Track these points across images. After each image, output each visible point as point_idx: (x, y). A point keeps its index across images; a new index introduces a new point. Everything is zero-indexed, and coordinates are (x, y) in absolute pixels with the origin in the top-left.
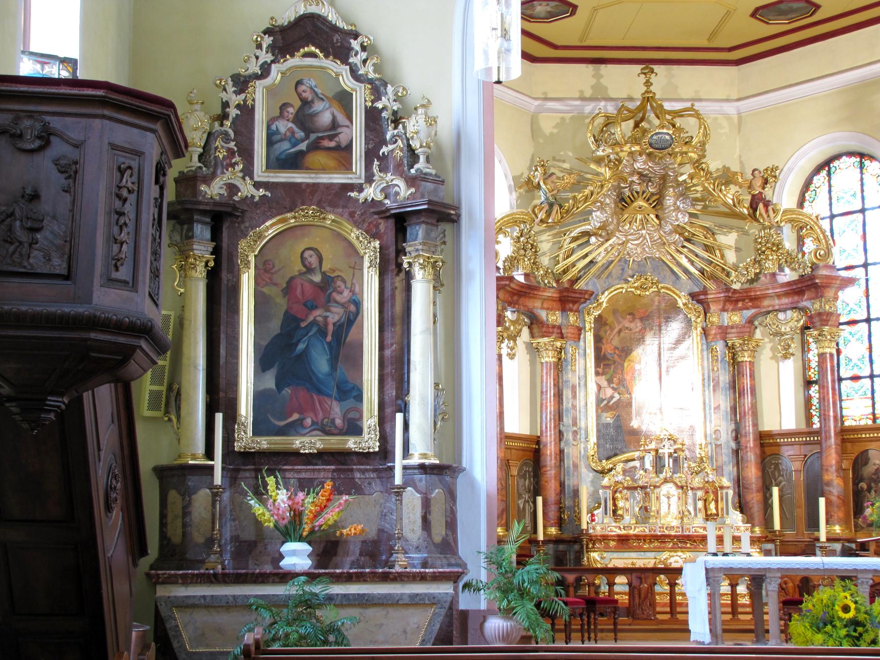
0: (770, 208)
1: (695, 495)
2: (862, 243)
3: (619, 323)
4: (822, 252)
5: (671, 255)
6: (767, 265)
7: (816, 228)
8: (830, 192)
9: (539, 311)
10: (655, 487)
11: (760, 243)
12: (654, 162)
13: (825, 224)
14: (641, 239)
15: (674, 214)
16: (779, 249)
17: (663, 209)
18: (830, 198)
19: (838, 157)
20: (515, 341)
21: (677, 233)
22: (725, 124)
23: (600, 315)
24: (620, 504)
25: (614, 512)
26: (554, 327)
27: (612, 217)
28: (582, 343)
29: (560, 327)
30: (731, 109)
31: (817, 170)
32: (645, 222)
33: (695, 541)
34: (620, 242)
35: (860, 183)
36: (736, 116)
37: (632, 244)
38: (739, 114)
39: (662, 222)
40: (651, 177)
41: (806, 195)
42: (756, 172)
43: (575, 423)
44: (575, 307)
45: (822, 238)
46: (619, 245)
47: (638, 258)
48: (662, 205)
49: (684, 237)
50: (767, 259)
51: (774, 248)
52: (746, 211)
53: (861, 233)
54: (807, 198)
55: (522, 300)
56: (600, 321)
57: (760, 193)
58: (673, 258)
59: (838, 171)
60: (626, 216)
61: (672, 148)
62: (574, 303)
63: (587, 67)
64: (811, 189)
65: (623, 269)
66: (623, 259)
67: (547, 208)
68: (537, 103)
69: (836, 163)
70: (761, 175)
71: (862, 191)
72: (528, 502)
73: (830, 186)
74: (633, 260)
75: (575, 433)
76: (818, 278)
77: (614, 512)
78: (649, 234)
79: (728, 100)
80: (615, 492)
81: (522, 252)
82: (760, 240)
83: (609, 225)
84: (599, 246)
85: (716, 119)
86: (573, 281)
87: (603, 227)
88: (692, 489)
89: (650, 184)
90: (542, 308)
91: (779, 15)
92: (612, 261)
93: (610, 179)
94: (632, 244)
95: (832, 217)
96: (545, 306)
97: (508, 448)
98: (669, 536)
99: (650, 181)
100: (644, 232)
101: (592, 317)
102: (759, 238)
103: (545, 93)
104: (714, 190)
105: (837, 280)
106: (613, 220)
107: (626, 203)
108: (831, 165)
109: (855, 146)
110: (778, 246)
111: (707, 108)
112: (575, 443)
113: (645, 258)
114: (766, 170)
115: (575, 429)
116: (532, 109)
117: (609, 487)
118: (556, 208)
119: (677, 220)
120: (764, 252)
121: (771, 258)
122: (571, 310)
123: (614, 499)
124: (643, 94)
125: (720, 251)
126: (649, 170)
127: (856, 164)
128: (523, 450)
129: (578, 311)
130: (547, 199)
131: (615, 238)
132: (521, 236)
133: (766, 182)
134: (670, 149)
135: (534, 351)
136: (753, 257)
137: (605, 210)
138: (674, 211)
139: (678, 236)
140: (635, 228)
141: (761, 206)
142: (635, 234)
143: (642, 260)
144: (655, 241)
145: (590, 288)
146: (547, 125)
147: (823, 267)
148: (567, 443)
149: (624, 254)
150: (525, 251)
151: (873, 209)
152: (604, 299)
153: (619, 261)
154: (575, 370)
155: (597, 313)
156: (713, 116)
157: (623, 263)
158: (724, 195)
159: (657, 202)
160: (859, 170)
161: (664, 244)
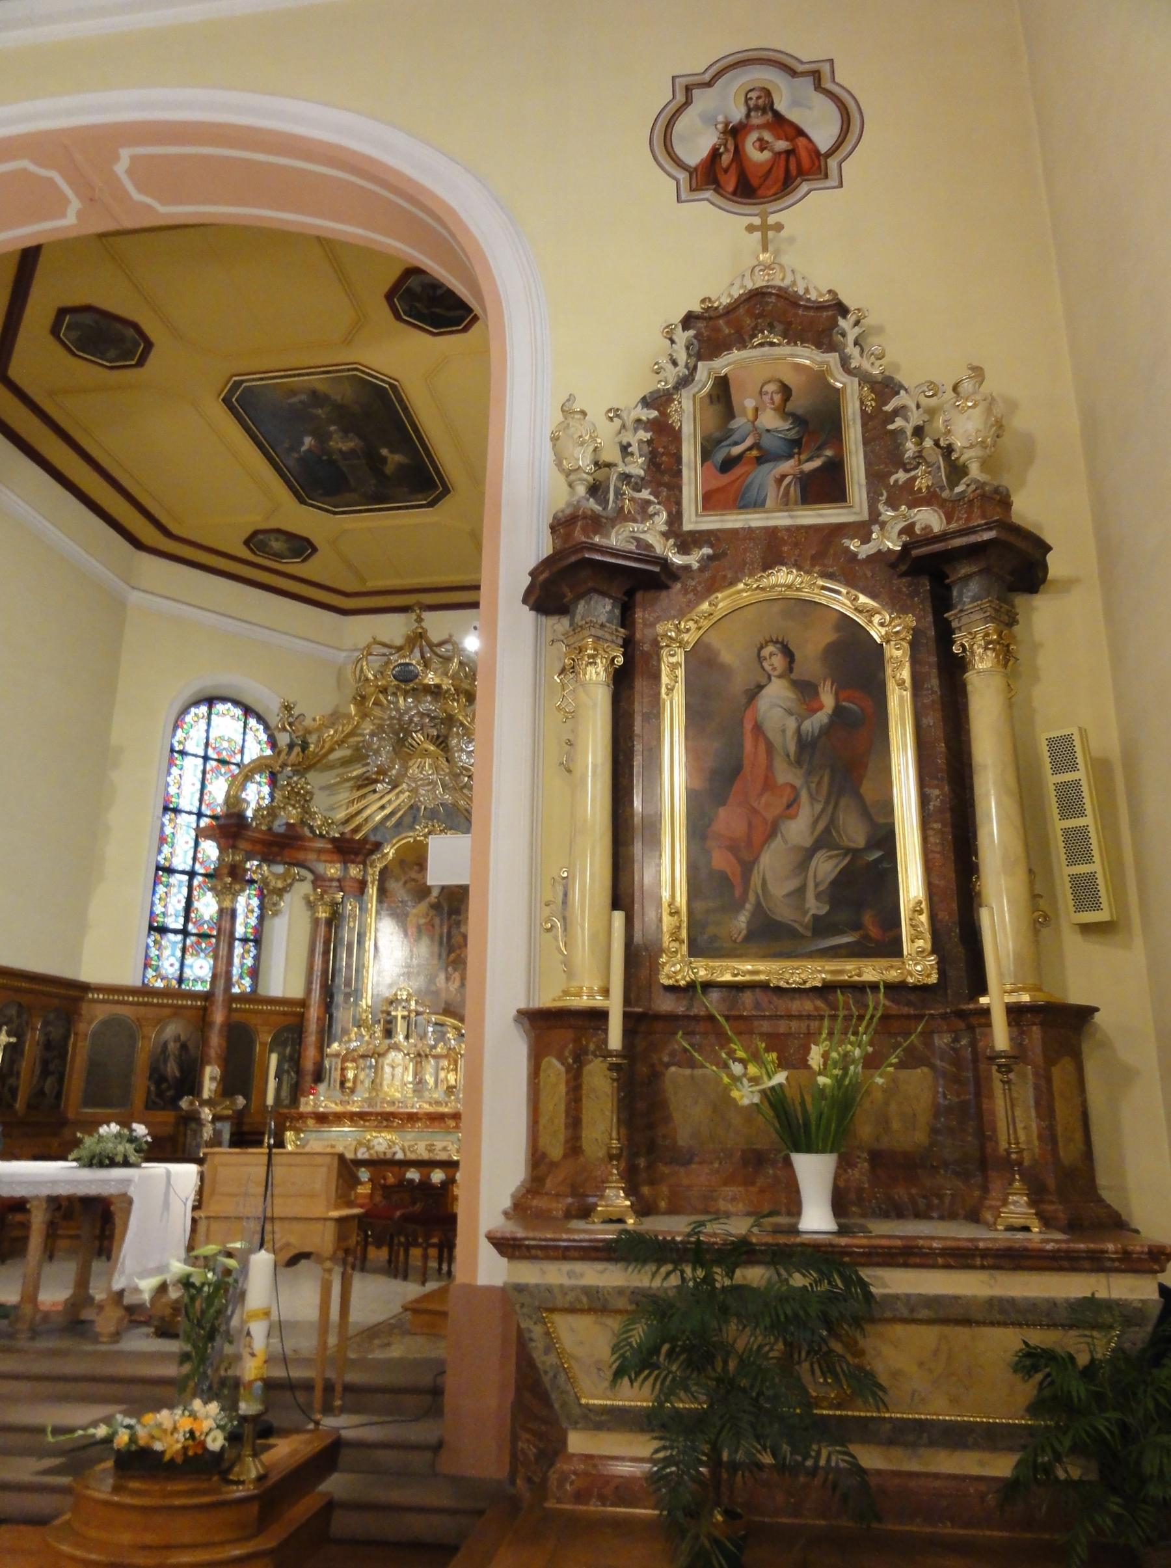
1: (437, 1064)
3: (405, 873)
9: (314, 863)
10: (380, 1055)
20: (281, 896)
21: (465, 776)
23: (386, 867)
24: (350, 1074)
25: (342, 1083)
26: (331, 880)
28: (365, 897)
29: (339, 880)
32: (437, 769)
33: (401, 1119)
43: (348, 984)
44: (360, 858)
55: (286, 852)
56: (383, 872)
62: (357, 854)
65: (415, 818)
68: (344, 654)
72: (288, 1072)
75: (347, 996)
77: (342, 1083)
80: (344, 1060)
84: (388, 793)
86: (356, 830)
88: (435, 1057)
90: (318, 860)
96: (323, 857)
97: (230, 1010)
98: (370, 1114)
101: (378, 870)
112: (346, 1006)
115: (348, 990)
117: (337, 1055)
118: (297, 749)
119: (461, 761)
122: (353, 862)
123: (343, 1069)
128: (284, 1014)
129: (364, 864)
134: (417, 680)
135: (311, 905)
138: (458, 751)
139: (466, 779)
145: (378, 838)
148: (337, 1007)
152: (390, 851)
153: (411, 807)
154: (354, 927)
155: (379, 866)
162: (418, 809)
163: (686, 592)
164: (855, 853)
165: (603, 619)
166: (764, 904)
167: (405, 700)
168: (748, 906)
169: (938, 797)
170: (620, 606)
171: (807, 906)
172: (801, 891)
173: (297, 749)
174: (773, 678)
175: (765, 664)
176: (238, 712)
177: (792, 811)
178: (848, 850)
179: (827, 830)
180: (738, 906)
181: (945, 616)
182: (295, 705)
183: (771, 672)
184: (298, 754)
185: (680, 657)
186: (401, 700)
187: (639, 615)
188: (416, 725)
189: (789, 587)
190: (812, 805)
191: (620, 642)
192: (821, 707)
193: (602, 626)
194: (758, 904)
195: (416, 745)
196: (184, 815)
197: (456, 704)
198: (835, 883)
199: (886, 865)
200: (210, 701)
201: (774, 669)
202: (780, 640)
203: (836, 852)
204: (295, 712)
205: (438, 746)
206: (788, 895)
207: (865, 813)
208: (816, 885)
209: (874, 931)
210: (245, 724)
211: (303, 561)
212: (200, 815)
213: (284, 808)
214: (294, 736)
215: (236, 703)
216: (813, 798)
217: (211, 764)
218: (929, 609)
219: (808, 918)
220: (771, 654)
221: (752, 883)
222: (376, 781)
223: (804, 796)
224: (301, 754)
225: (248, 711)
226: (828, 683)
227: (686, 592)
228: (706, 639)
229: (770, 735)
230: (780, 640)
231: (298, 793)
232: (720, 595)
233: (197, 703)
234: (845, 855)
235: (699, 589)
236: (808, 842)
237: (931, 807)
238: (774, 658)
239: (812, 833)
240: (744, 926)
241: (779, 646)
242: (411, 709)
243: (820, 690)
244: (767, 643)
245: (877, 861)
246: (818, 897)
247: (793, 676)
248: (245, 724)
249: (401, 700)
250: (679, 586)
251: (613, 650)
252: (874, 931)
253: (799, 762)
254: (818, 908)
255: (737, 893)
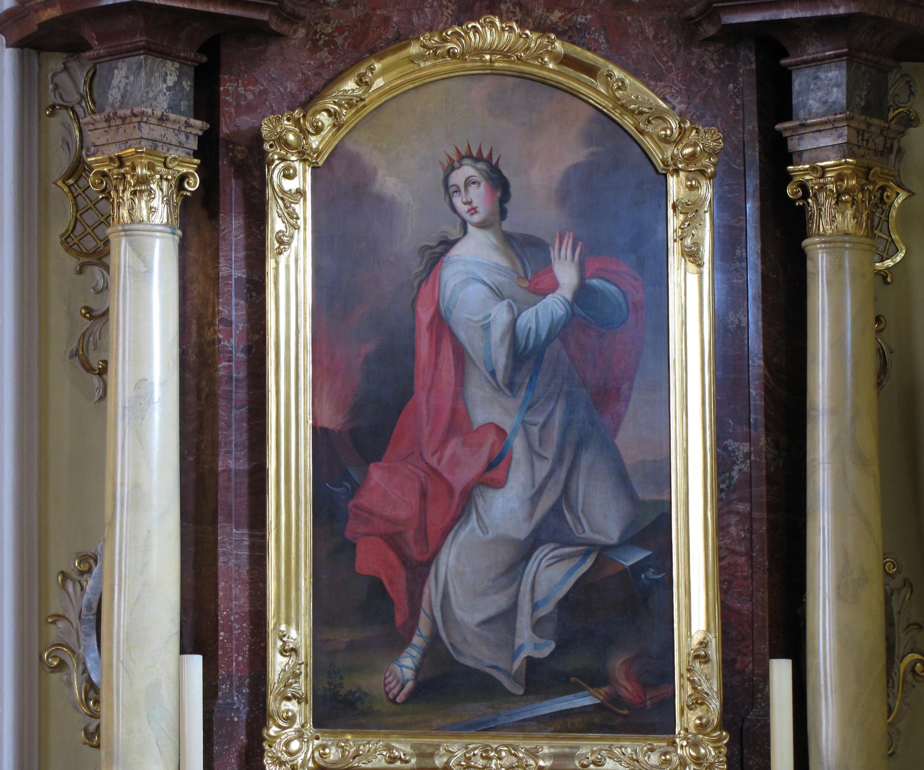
163: (315, 48)
164: (603, 551)
165: (162, 104)
166: (443, 635)
168: (417, 640)
169: (748, 455)
170: (192, 74)
171: (518, 642)
172: (508, 617)
174: (471, 228)
175: (458, 201)
177: (495, 474)
178: (591, 547)
179: (556, 510)
180: (400, 642)
181: (778, 127)
183: (467, 217)
185: (302, 180)
187: (228, 87)
189: (506, 54)
190: (532, 465)
191: (193, 144)
192: (554, 286)
193: (162, 119)
194: (435, 637)
198: (565, 604)
199: (651, 574)
201: (473, 211)
202: (485, 154)
203: (568, 550)
206: (487, 622)
207: (622, 478)
208: (535, 607)
209: (627, 688)
216: (533, 453)
218: (752, 108)
219: (517, 664)
220: (468, 182)
221: (425, 604)
223: (518, 446)
226: (568, 242)
227: (315, 48)
228: (351, 146)
229: (462, 336)
230: (485, 154)
232: (378, 66)
234: (586, 554)
235: (339, 40)
236: (522, 531)
237: (735, 474)
238: (473, 189)
239: (531, 516)
240: (409, 674)
241: (481, 165)
243: (554, 254)
244: (461, 158)
245: (639, 567)
246: (537, 626)
247: (506, 226)
250: (301, 33)
251: (182, 162)
252: (627, 688)
253: (511, 386)
254: (536, 647)
255: (400, 618)
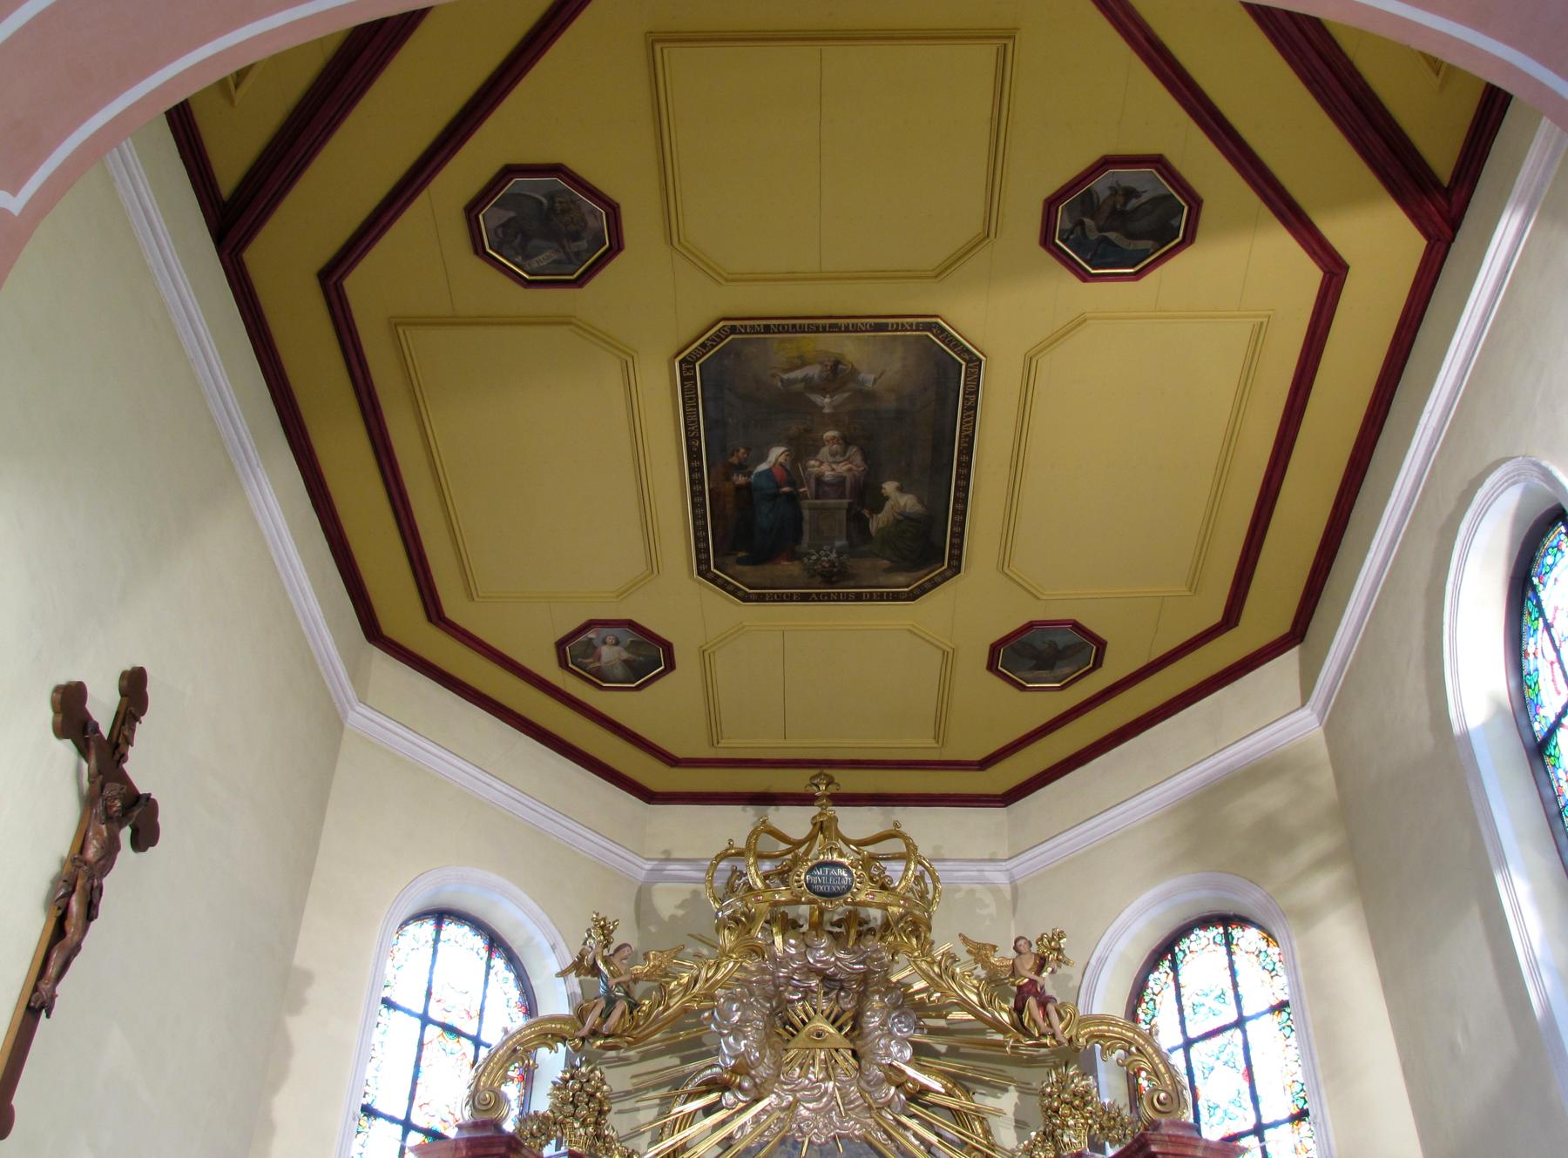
0: (1051, 1007)
2: (1246, 1085)
4: (1162, 1095)
5: (885, 1132)
6: (1066, 1139)
7: (1150, 1050)
8: (1179, 997)
11: (1050, 1095)
12: (845, 949)
13: (1178, 1060)
14: (825, 1100)
15: (882, 1041)
16: (1086, 1104)
17: (861, 1036)
18: (1181, 1010)
19: (1184, 931)
21: (891, 1082)
22: (988, 899)
27: (761, 1049)
30: (997, 876)
31: (1152, 963)
34: (784, 1104)
35: (1228, 972)
36: (1008, 888)
37: (808, 1109)
38: (1013, 882)
39: (863, 1062)
40: (841, 981)
41: (1139, 1011)
42: (1021, 942)
45: (1163, 1070)
46: (783, 1109)
47: (820, 1138)
48: (861, 1028)
49: (906, 1093)
50: (1064, 1125)
51: (1077, 1102)
52: (1005, 1018)
53: (1242, 1065)
54: (1142, 1016)
57: (1033, 982)
58: (890, 1137)
59: (1189, 956)
60: (792, 1053)
61: (853, 894)
63: (744, 810)
64: (1147, 999)
66: (790, 1141)
67: (602, 1004)
69: (1184, 944)
70: (1034, 949)
71: (1235, 985)
73: (1178, 987)
74: (810, 1142)
76: (1154, 1142)
78: (839, 1089)
79: (991, 860)
81: (571, 1108)
82: (1049, 1090)
83: (753, 1066)
85: (972, 892)
87: (741, 1068)
89: (842, 994)
91: (1038, 667)
92: (768, 1142)
93: (732, 950)
94: (808, 1109)
95: (1188, 1044)
99: (842, 988)
100: (831, 1084)
102: (1047, 1086)
103: (665, 852)
104: (940, 976)
105: (1196, 1147)
106: (763, 1056)
107: (792, 1025)
108: (1177, 949)
109: (1209, 901)
110: (1083, 1098)
111: (956, 874)
113: (834, 1138)
114: (1041, 939)
116: (642, 876)
118: (621, 1006)
119: (889, 1055)
120: (1056, 1111)
121: (1071, 1122)
124: (814, 818)
125: (982, 1120)
126: (836, 966)
127: (1218, 939)
130: (609, 990)
131: (774, 1096)
132: (572, 1077)
133: (1041, 964)
136: (1042, 1128)
137: (744, 1033)
138: (881, 1037)
139: (893, 1089)
140: (811, 1076)
141: (1032, 1002)
142: (812, 1089)
143: (827, 1142)
144: (851, 1102)
146: (667, 902)
147: (1166, 1125)
149: (790, 1129)
150: (576, 1107)
151: (1257, 1016)
153: (783, 1141)
156: (965, 887)
157: (789, 1149)
158: (961, 987)
159: (854, 1026)
160: (1223, 949)
161: (870, 1108)
162: (797, 1145)
167: (785, 942)
173: (621, 1006)
176: (479, 943)
182: (615, 927)
184: (623, 1013)
186: (778, 939)
188: (796, 987)
195: (799, 1024)
196: (381, 1120)
197: (914, 941)
200: (440, 915)
204: (618, 938)
205: (840, 1029)
210: (489, 967)
211: (638, 688)
212: (407, 1126)
213: (562, 1124)
214: (612, 982)
215: (478, 926)
217: (432, 1031)
222: (725, 1087)
224: (628, 1017)
225: (496, 943)
231: (592, 1096)
233: (419, 916)
242: (792, 957)
248: (489, 967)
249: (778, 939)
